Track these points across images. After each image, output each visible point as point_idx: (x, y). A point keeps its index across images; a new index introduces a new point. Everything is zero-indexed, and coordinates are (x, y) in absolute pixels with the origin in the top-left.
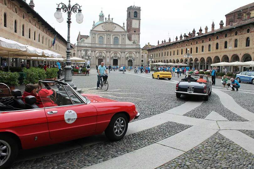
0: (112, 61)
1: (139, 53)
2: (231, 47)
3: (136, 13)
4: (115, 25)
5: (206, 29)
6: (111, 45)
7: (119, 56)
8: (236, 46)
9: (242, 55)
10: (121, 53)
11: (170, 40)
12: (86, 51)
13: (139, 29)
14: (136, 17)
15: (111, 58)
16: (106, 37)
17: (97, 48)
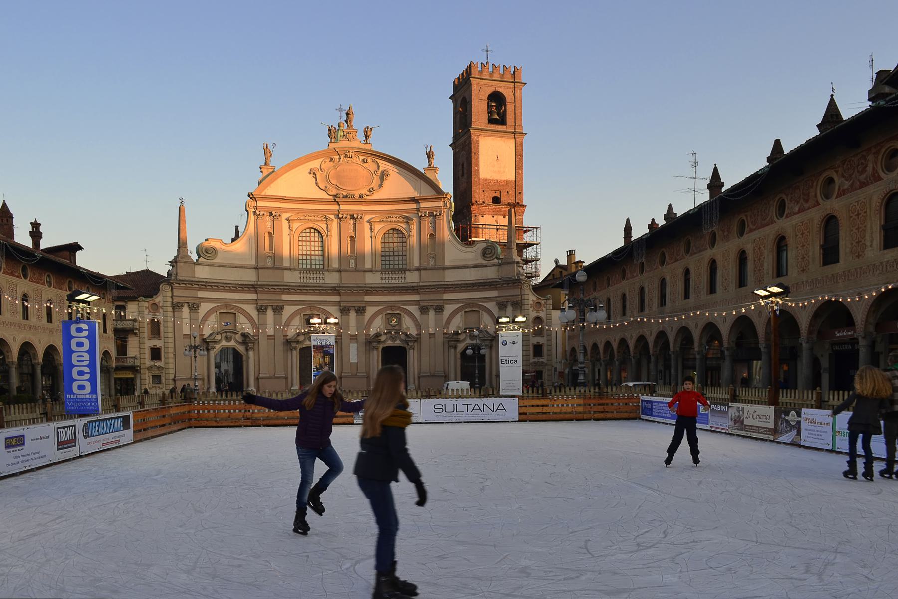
0: (376, 359)
3: (497, 99)
4: (384, 165)
6: (368, 275)
7: (413, 332)
10: (424, 310)
13: (517, 185)
14: (502, 121)
15: (371, 342)
17: (288, 288)
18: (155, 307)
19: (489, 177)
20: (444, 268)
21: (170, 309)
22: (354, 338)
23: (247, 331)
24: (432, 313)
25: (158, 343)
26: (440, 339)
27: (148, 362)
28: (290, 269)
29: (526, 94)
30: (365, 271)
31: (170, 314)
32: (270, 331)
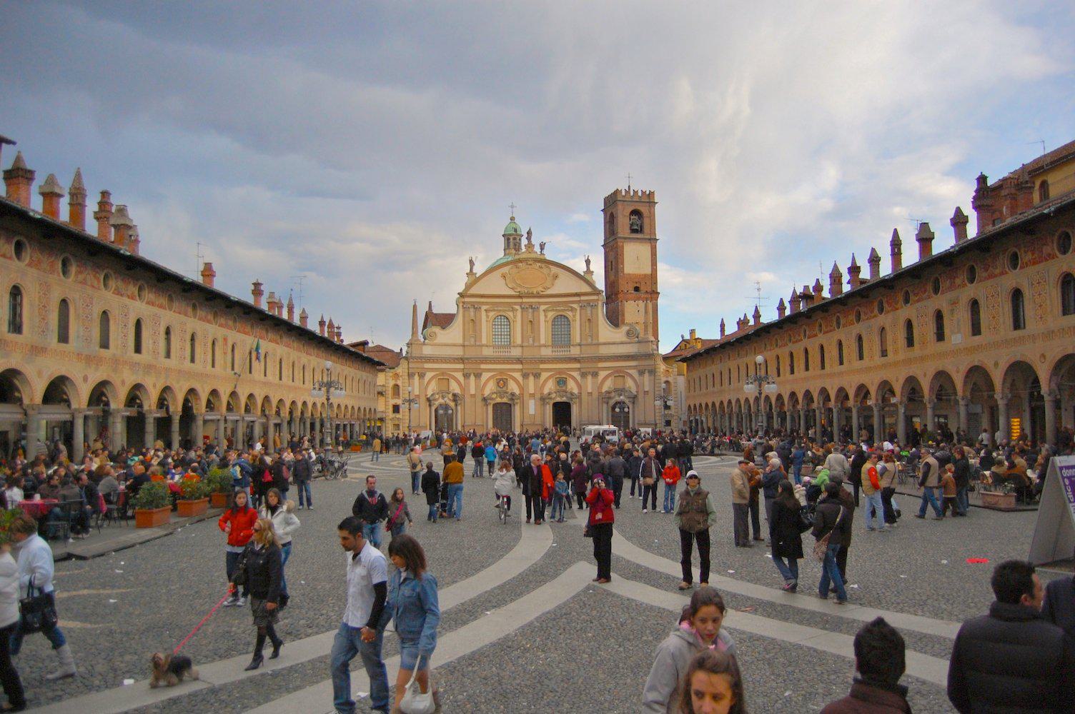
0: (549, 410)
1: (653, 372)
2: (957, 336)
4: (554, 270)
5: (874, 260)
7: (576, 391)
8: (976, 330)
9: (1003, 366)
10: (584, 375)
11: (757, 315)
12: (444, 378)
13: (653, 277)
16: (519, 314)
18: (397, 376)
19: (631, 272)
20: (599, 344)
21: (407, 377)
22: (532, 396)
23: (456, 392)
24: (589, 378)
25: (399, 402)
26: (595, 395)
27: (391, 414)
28: (487, 346)
29: (658, 209)
30: (540, 346)
31: (407, 381)
32: (473, 392)
